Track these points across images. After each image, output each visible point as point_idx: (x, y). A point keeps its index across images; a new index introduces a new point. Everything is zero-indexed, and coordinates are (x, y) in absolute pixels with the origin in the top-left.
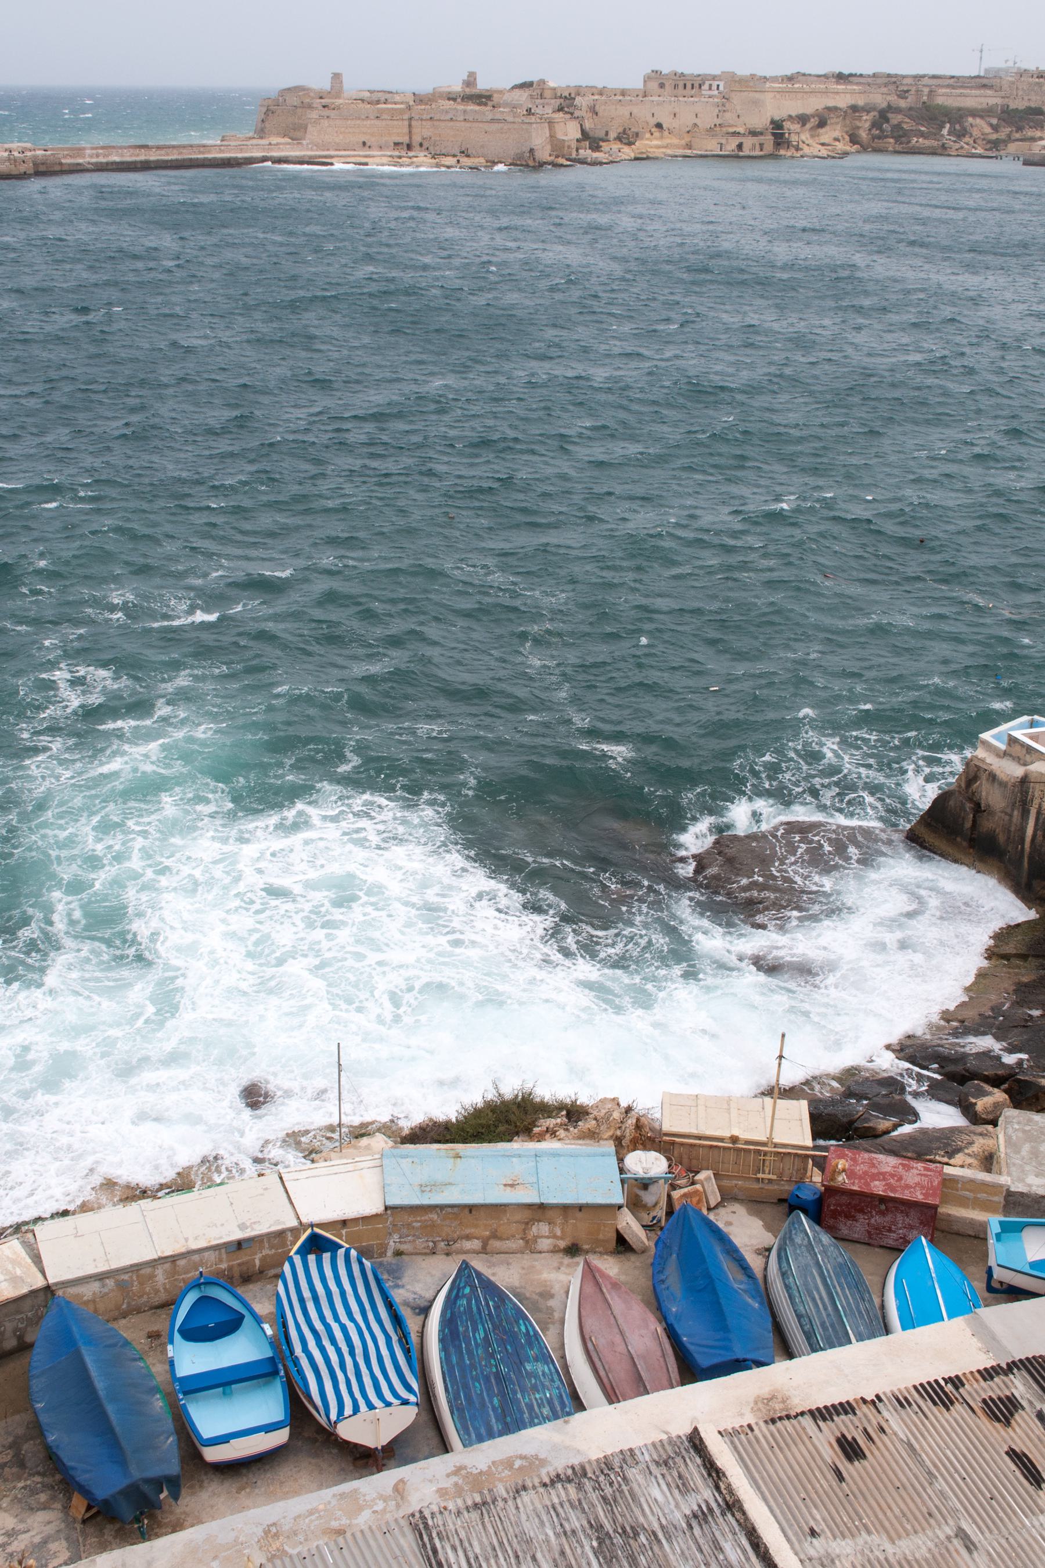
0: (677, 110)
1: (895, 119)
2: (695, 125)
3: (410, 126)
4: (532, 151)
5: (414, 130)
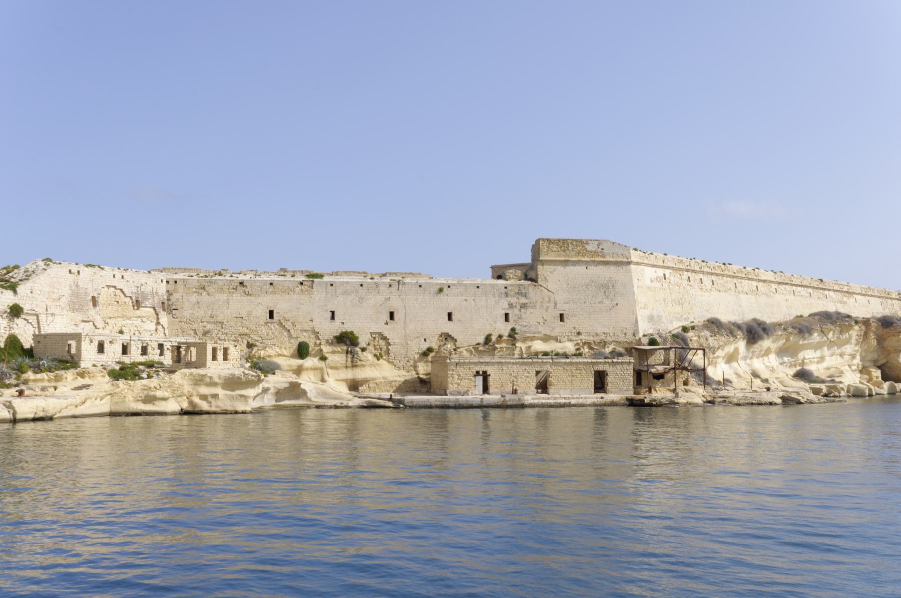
2: (447, 337)
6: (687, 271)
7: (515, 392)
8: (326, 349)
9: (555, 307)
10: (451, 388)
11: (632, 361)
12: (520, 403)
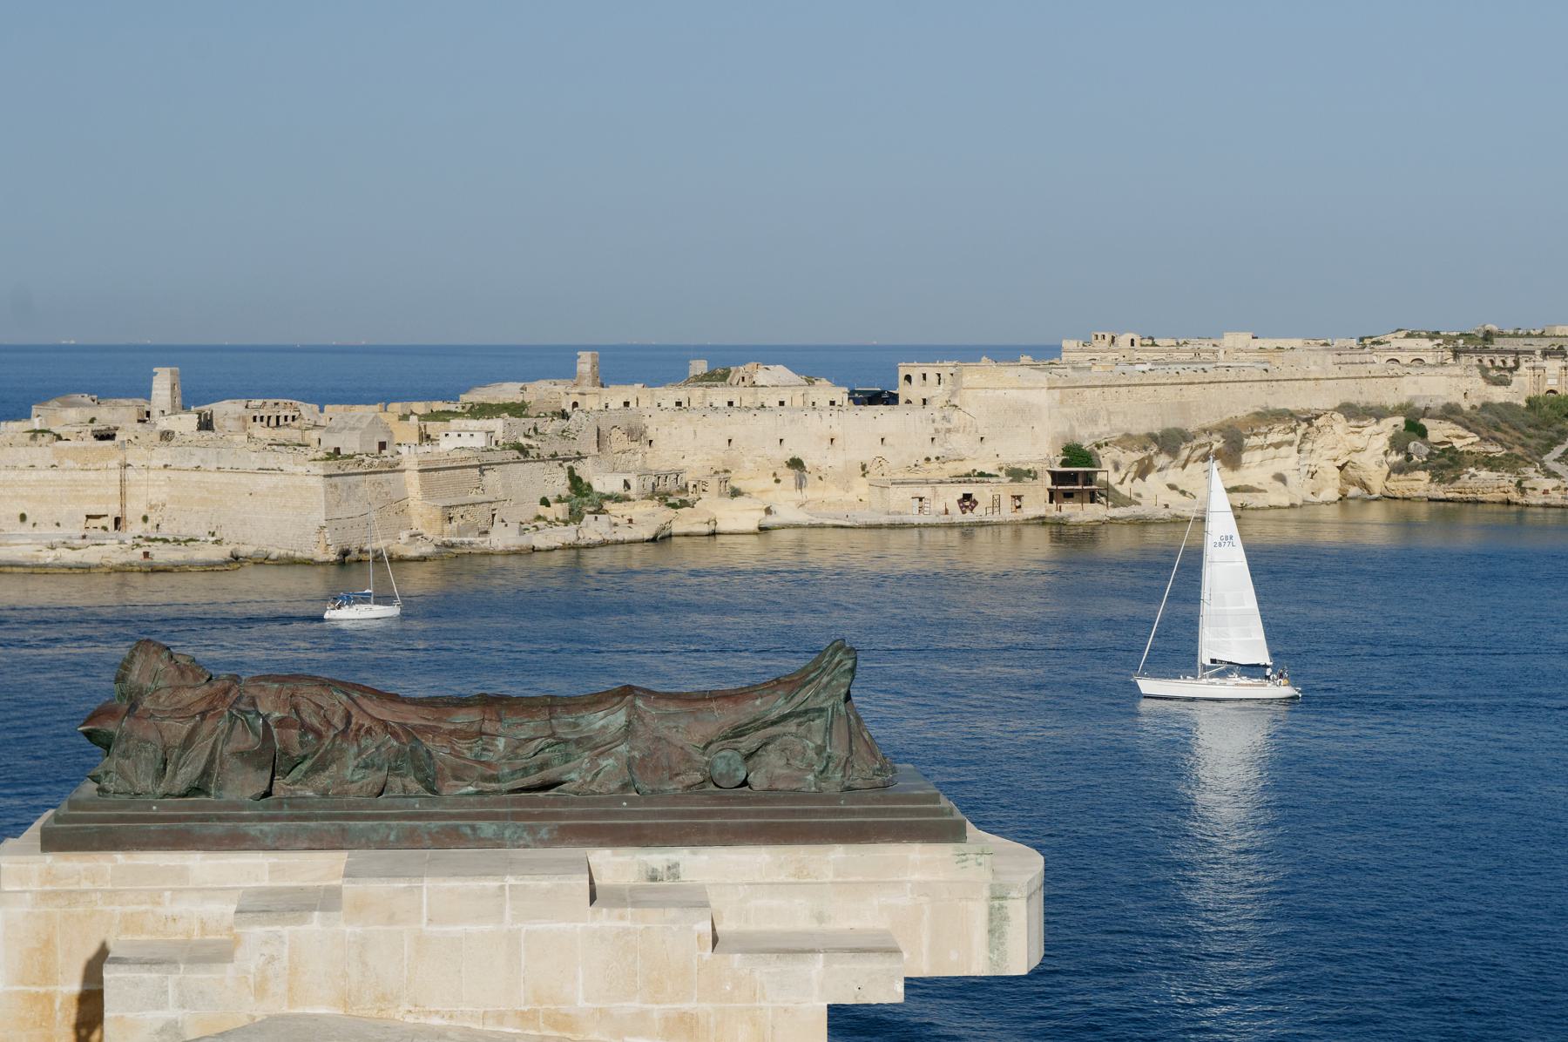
0: (837, 431)
1: (1438, 431)
5: (130, 491)
6: (1103, 386)
7: (947, 512)
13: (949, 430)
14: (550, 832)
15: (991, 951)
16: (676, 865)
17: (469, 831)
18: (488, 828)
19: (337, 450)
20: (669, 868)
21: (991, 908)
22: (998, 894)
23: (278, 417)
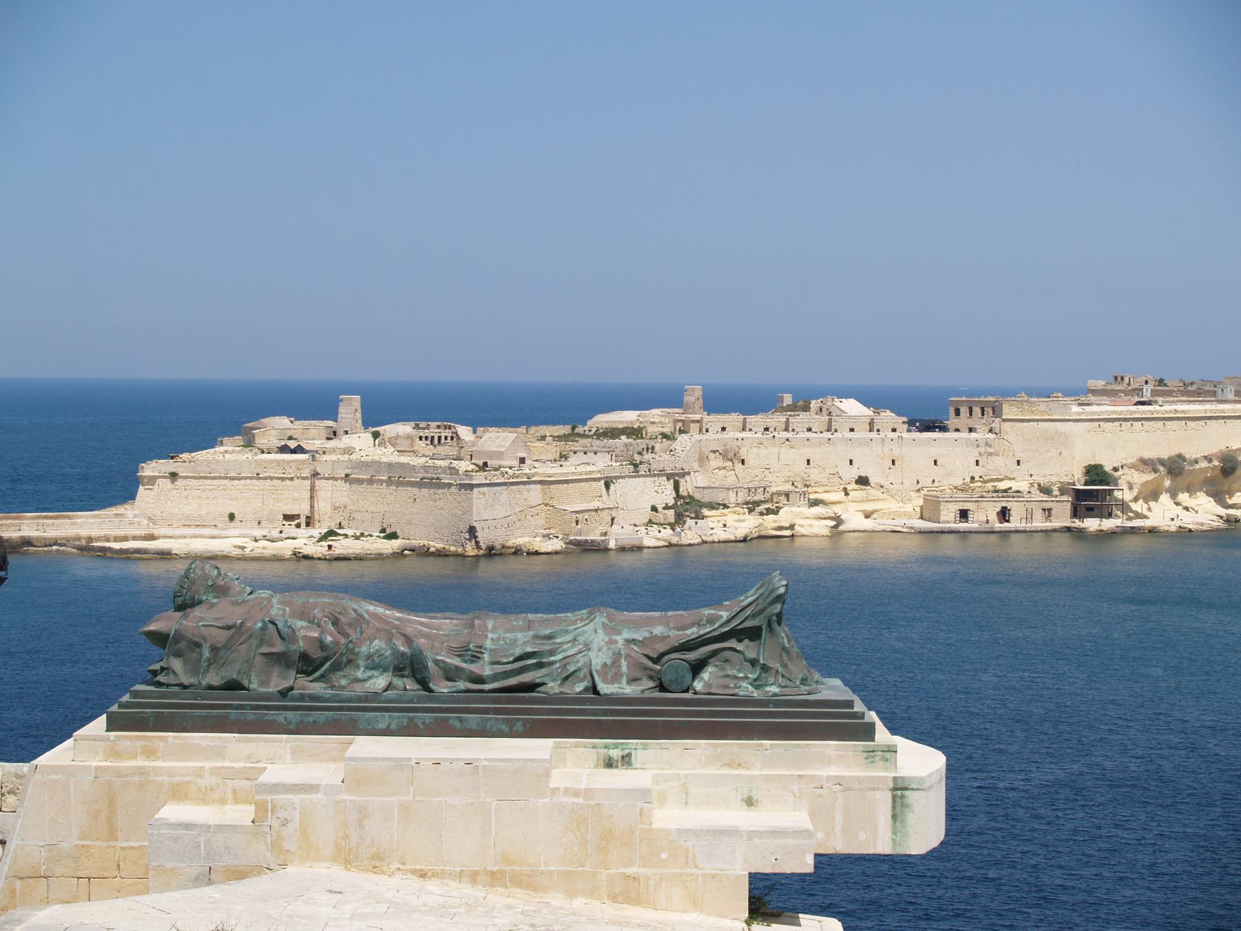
3: (312, 489)
4: (472, 530)
7: (987, 522)
8: (849, 487)
9: (1014, 455)
10: (942, 518)
11: (1070, 499)
12: (991, 530)
13: (990, 454)
14: (524, 725)
15: (894, 833)
16: (629, 755)
17: (457, 724)
18: (473, 720)
19: (485, 464)
20: (623, 757)
21: (894, 797)
22: (900, 785)
23: (440, 438)
